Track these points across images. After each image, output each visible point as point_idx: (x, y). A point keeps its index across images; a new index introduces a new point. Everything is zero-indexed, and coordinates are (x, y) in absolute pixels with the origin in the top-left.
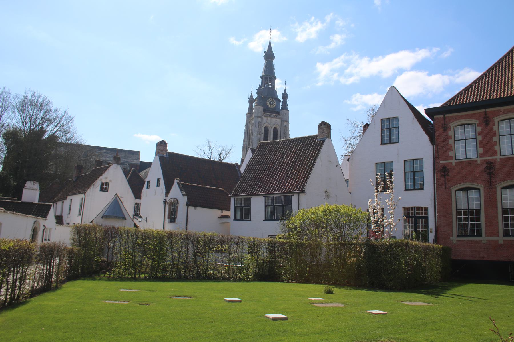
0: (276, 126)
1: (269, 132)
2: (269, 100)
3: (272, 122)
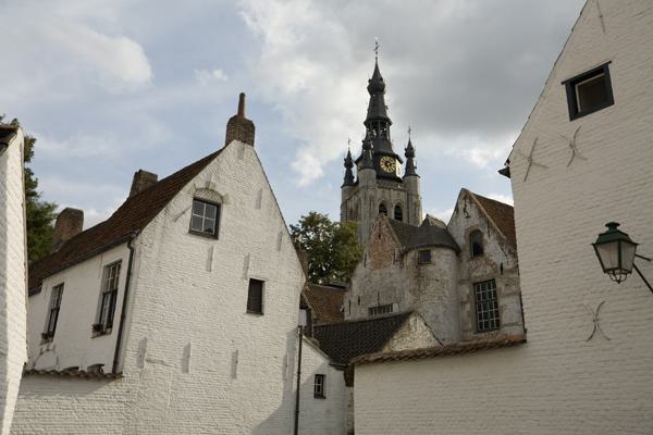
3: (394, 196)
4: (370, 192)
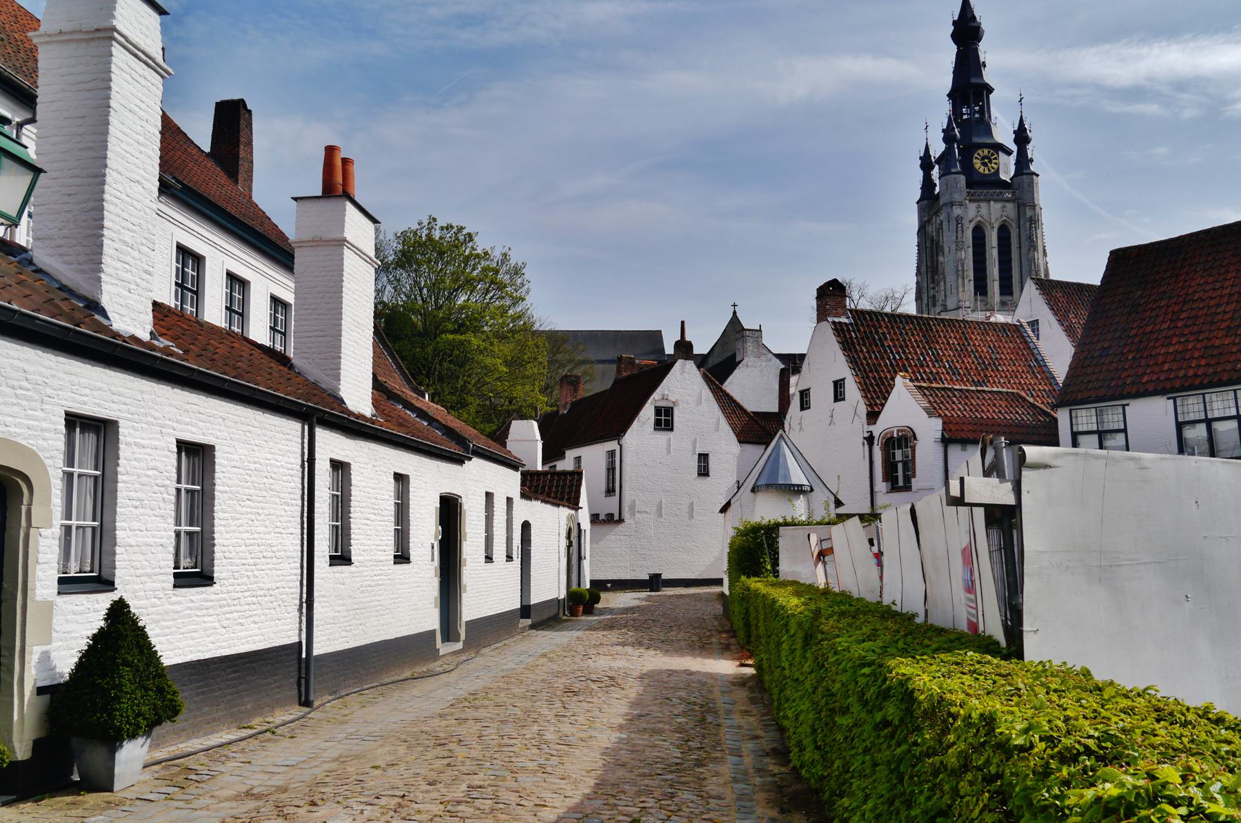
0: (1005, 220)
1: (987, 240)
2: (978, 154)
3: (994, 212)
4: (957, 211)
